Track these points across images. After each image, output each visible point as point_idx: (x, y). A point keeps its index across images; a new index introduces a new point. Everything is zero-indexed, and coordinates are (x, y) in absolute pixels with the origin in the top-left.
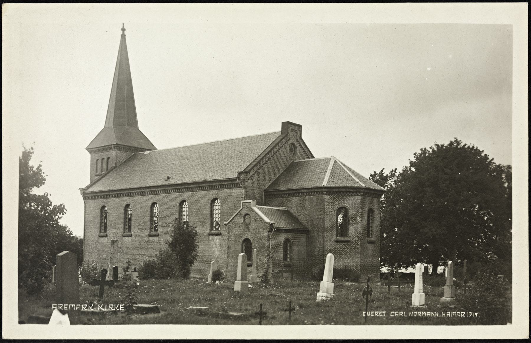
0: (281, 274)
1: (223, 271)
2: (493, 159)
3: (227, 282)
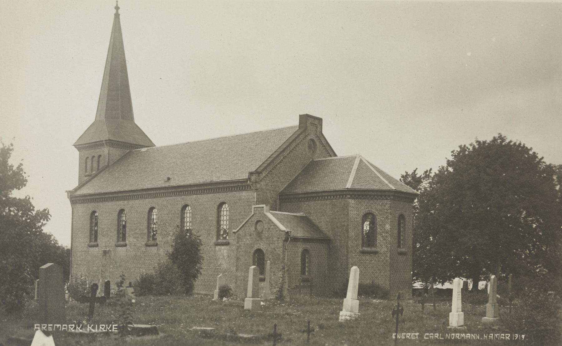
0: (298, 290)
1: (232, 286)
2: (543, 158)
3: (236, 299)
